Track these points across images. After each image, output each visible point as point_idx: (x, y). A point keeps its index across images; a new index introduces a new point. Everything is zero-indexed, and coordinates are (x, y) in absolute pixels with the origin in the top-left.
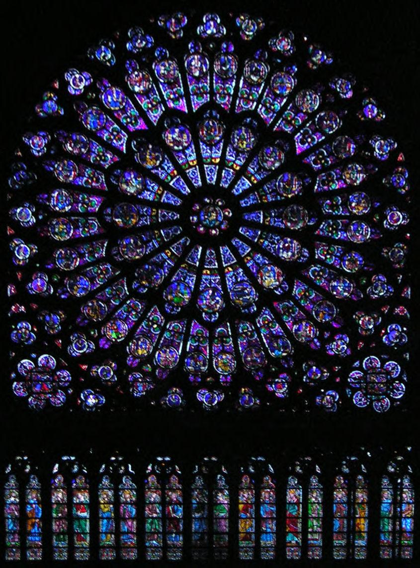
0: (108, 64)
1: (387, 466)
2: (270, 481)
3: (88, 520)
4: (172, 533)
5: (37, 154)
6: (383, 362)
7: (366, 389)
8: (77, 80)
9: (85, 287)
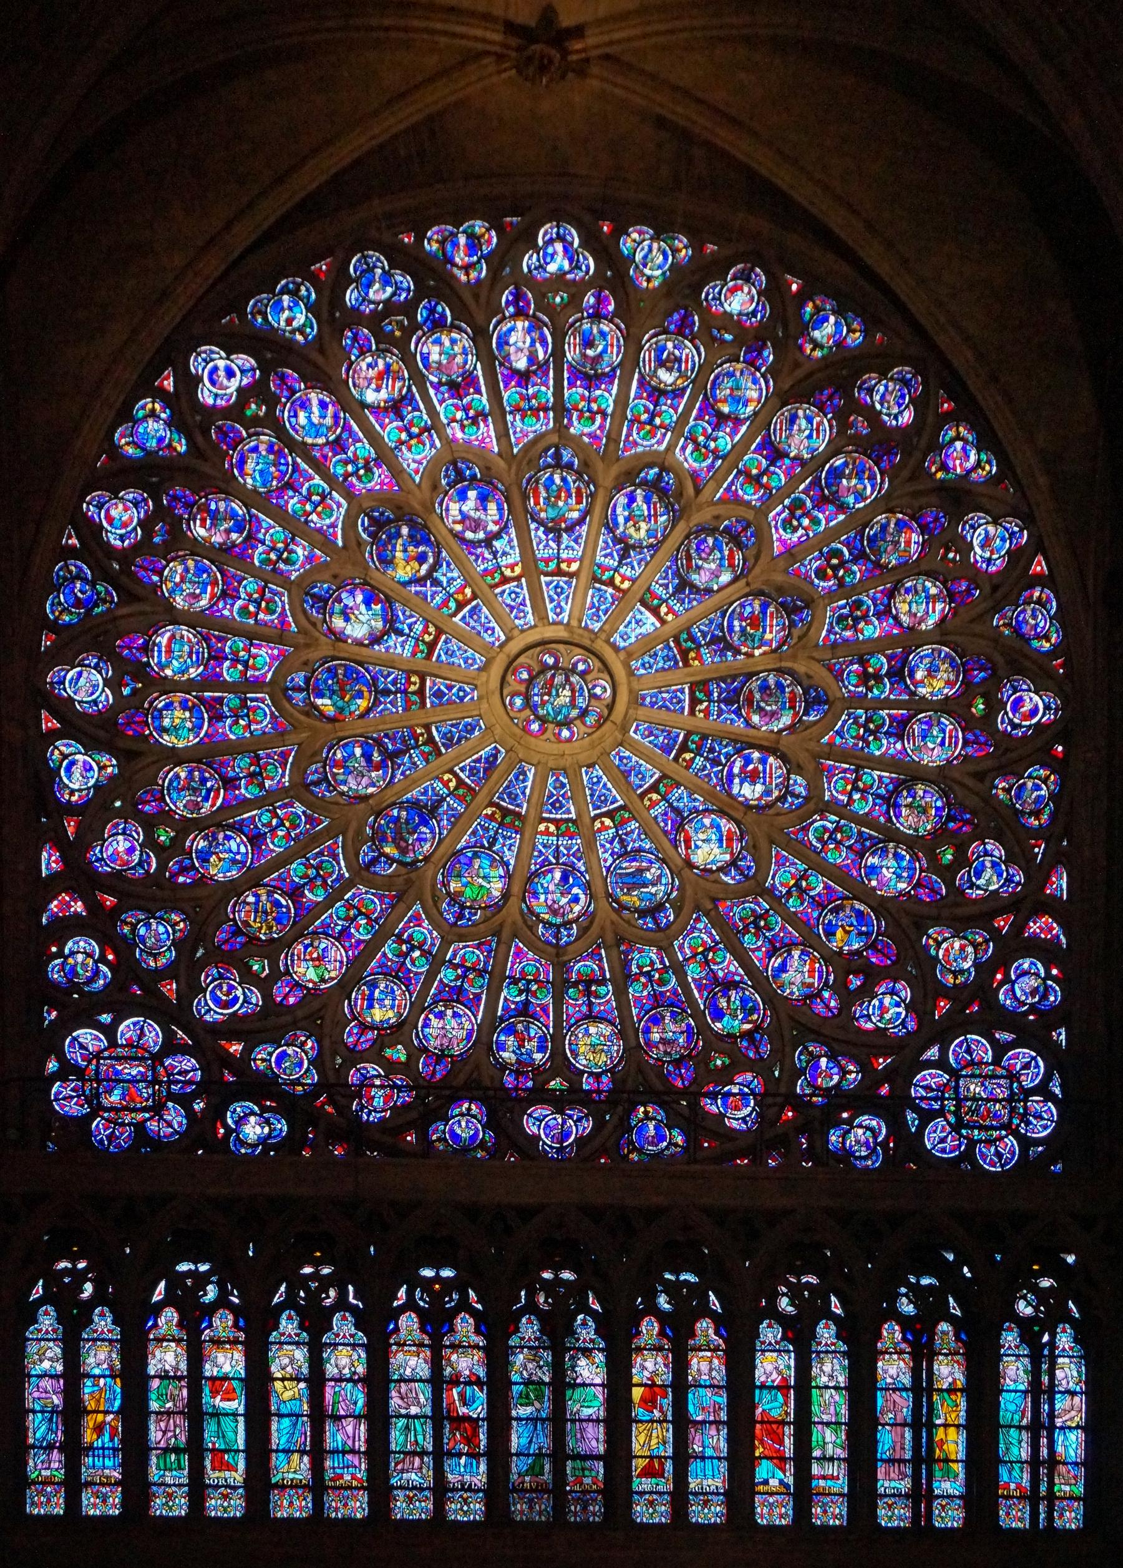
0: (299, 337)
1: (1013, 1302)
2: (711, 1331)
3: (241, 1419)
4: (459, 1455)
5: (118, 543)
6: (1001, 1051)
8: (222, 373)
9: (238, 857)
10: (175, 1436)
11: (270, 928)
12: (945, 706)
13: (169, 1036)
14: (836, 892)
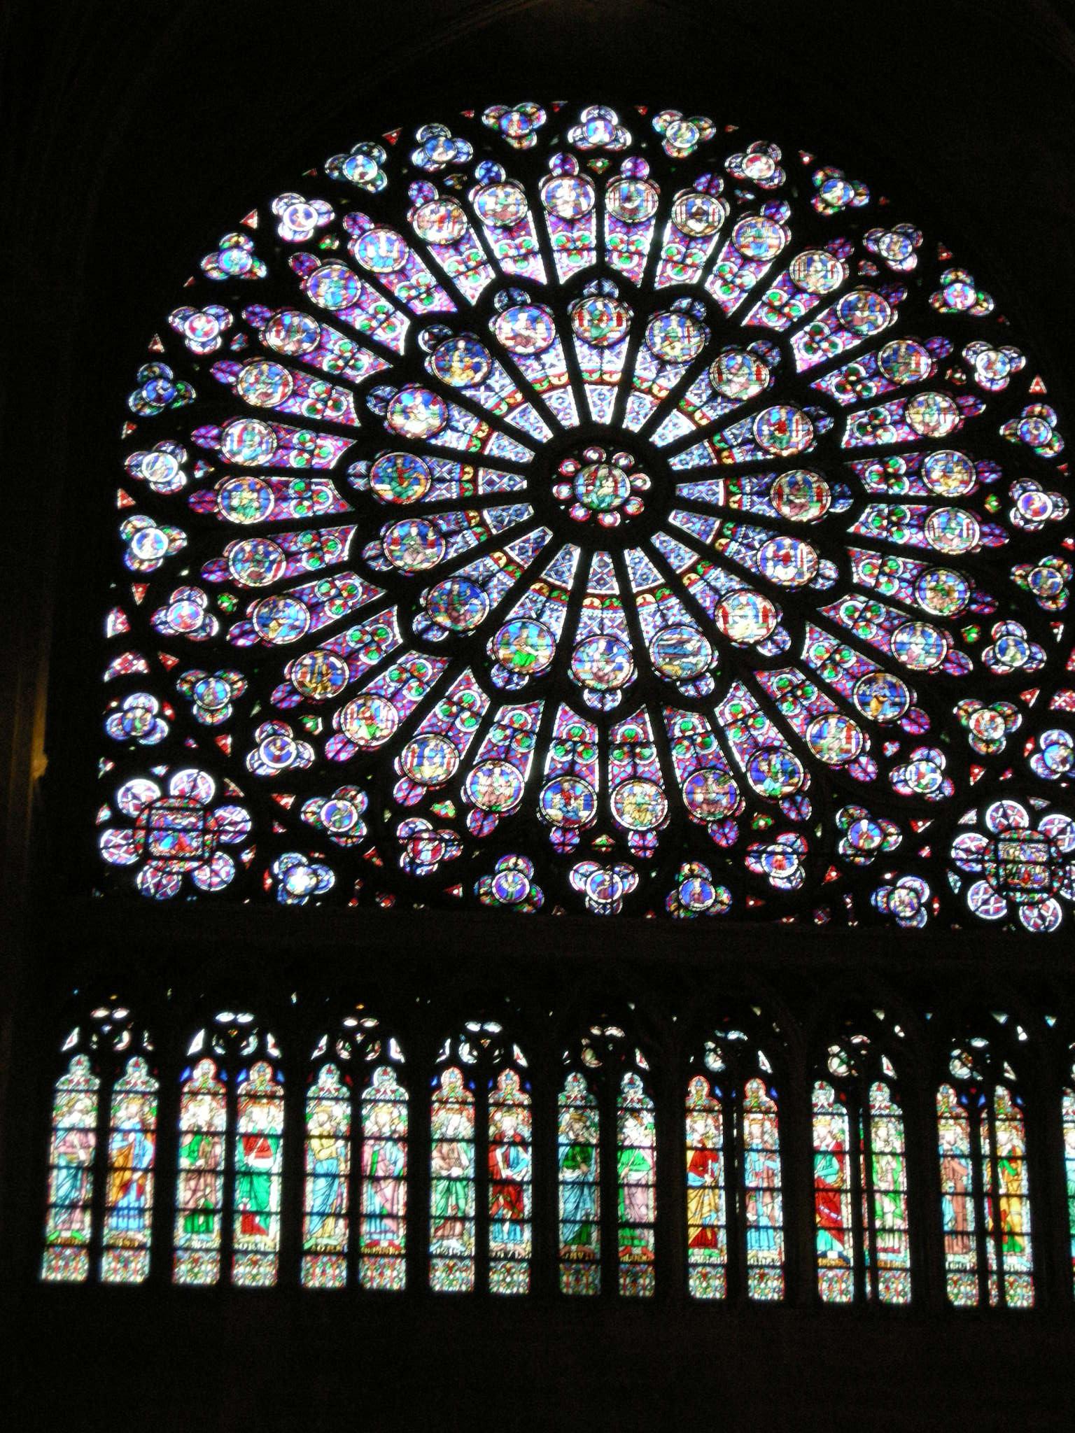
0: (370, 188)
2: (762, 1092)
6: (1036, 815)
7: (996, 875)
8: (301, 214)
9: (297, 623)
10: (205, 1196)
11: (325, 688)
12: (960, 503)
13: (221, 787)
14: (868, 664)
